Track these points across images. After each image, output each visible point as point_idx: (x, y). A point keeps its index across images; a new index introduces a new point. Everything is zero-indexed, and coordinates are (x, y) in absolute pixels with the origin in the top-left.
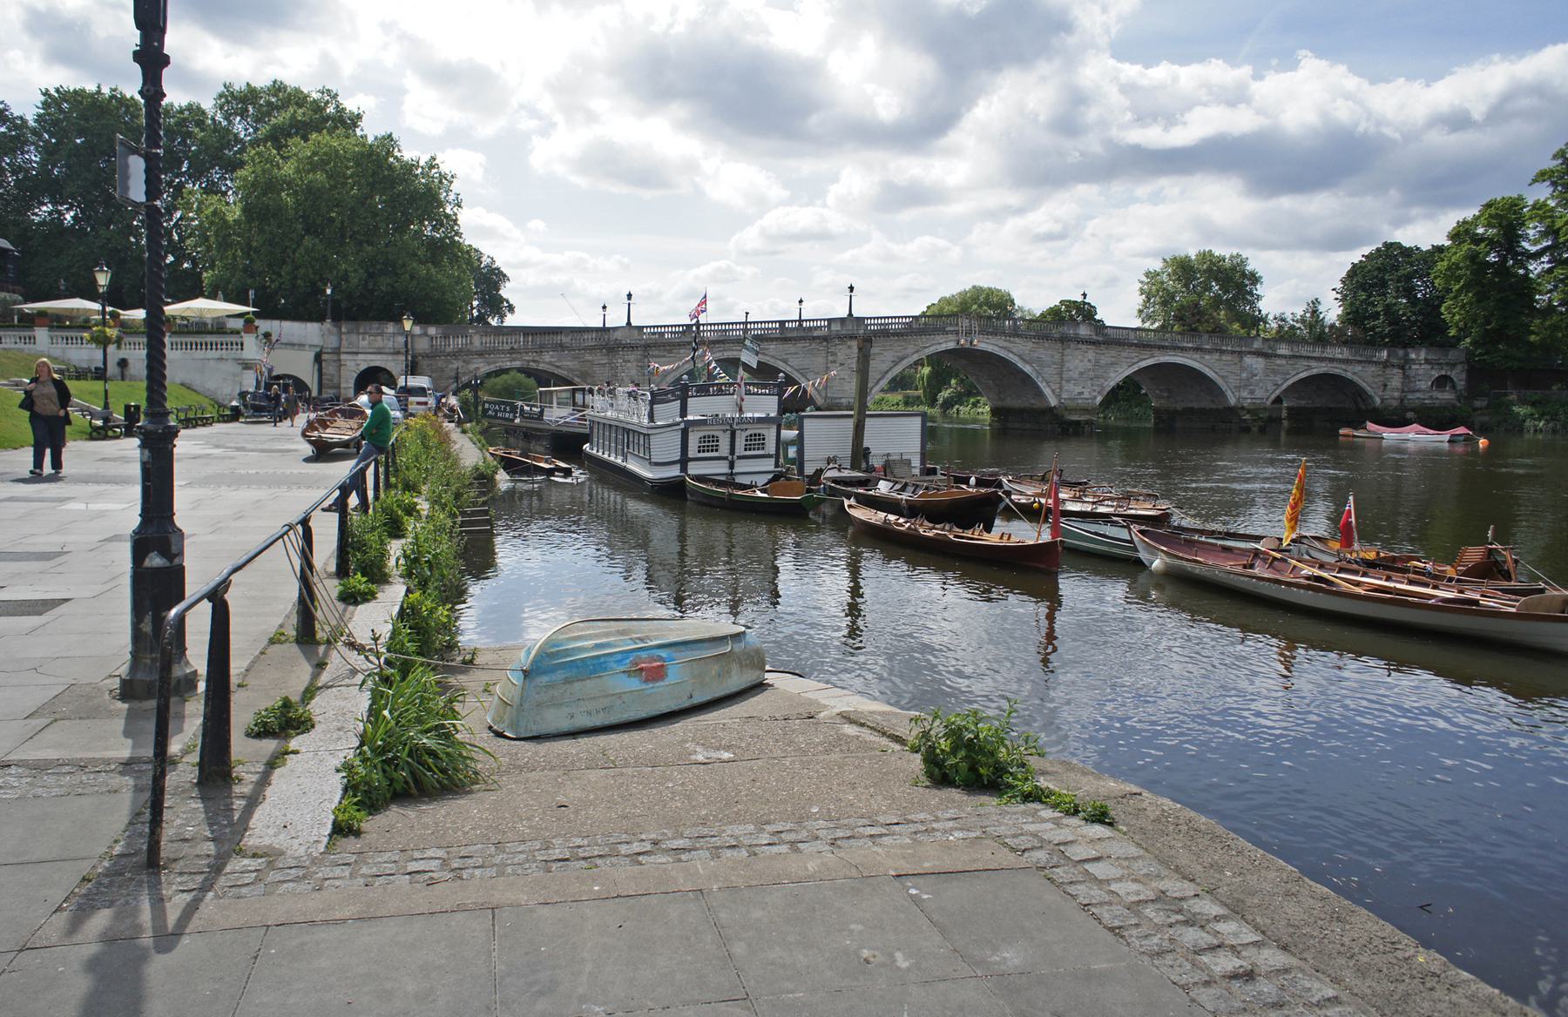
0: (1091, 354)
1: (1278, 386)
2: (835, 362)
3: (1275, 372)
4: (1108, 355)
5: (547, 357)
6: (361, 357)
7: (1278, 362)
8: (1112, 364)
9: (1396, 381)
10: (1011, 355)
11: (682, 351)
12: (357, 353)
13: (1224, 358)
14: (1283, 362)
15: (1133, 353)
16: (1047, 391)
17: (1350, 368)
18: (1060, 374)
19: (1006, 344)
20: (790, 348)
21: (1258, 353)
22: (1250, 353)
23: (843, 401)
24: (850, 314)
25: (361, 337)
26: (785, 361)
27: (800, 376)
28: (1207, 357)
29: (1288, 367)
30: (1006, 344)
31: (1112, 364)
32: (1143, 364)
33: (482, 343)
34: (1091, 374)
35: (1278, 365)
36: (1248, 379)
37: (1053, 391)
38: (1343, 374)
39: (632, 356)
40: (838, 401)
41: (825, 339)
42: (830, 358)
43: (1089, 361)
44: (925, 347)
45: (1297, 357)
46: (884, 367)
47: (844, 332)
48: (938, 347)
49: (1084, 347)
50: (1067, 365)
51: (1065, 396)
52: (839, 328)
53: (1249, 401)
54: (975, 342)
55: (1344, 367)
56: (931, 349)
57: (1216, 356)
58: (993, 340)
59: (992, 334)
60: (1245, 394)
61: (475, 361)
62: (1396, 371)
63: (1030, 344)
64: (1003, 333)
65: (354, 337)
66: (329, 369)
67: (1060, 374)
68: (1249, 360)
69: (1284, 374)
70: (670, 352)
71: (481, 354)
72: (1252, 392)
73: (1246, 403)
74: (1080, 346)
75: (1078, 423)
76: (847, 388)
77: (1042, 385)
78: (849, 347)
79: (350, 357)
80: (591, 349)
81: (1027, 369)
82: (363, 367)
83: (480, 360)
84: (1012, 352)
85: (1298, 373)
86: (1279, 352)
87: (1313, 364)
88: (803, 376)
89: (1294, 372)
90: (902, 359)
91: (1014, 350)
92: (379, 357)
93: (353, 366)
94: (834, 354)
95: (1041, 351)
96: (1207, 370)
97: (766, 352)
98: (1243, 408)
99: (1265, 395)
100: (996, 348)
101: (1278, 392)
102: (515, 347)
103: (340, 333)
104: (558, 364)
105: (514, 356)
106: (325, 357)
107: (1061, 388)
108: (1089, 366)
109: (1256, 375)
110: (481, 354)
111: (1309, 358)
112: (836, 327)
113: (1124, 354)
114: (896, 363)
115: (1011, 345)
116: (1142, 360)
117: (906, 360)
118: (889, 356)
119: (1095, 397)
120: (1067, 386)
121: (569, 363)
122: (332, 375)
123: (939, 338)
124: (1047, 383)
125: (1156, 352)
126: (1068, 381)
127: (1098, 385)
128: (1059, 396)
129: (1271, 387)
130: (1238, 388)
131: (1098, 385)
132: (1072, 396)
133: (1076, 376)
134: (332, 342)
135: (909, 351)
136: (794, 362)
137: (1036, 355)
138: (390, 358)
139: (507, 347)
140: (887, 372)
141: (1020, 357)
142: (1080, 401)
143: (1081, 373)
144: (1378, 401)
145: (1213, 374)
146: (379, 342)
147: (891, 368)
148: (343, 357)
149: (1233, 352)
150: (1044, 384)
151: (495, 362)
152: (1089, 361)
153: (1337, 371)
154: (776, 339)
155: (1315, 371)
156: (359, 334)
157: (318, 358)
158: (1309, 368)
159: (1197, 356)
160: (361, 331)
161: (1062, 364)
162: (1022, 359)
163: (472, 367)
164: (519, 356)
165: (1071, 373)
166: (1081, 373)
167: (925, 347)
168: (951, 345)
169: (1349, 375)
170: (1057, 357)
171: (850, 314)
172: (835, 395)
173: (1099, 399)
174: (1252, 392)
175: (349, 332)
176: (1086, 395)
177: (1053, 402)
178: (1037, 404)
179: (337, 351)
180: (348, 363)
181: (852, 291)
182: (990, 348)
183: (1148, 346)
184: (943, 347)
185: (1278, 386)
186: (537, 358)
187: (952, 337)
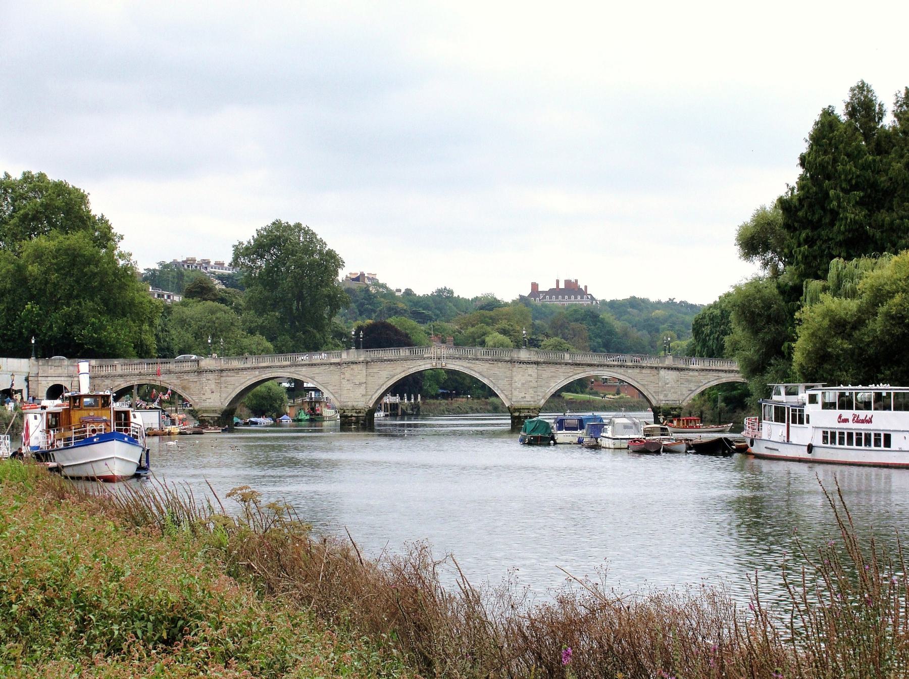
0: (532, 370)
1: (693, 391)
2: (344, 379)
3: (688, 381)
4: (548, 371)
5: (161, 378)
7: (691, 373)
11: (245, 373)
13: (644, 371)
14: (696, 373)
15: (569, 369)
19: (468, 365)
20: (316, 370)
23: (349, 403)
25: (49, 367)
27: (323, 388)
28: (630, 371)
29: (701, 378)
30: (468, 365)
33: (122, 370)
34: (534, 384)
35: (690, 376)
37: (506, 396)
39: (211, 376)
40: (346, 404)
41: (339, 364)
42: (342, 376)
43: (530, 375)
44: (409, 368)
45: (707, 370)
46: (381, 382)
47: (348, 360)
48: (419, 368)
49: (524, 366)
50: (515, 378)
52: (346, 357)
53: (664, 402)
56: (414, 369)
57: (638, 370)
58: (458, 362)
59: (457, 358)
60: (661, 397)
61: (119, 380)
63: (488, 365)
64: (467, 358)
68: (662, 372)
69: (694, 382)
70: (238, 373)
71: (121, 376)
72: (666, 396)
74: (521, 365)
79: (43, 379)
80: (187, 372)
81: (485, 381)
82: (51, 384)
83: (122, 380)
84: (472, 370)
86: (691, 366)
87: (722, 375)
89: (706, 381)
90: (394, 376)
91: (476, 369)
92: (59, 379)
93: (45, 385)
95: (496, 369)
97: (300, 373)
99: (681, 398)
100: (462, 368)
102: (142, 371)
103: (39, 365)
104: (167, 382)
105: (141, 377)
106: (30, 379)
107: (512, 394)
108: (529, 379)
109: (668, 384)
110: (121, 376)
111: (716, 370)
113: (561, 370)
114: (389, 379)
115: (472, 366)
117: (396, 377)
118: (384, 374)
119: (540, 400)
120: (516, 393)
121: (175, 381)
122: (34, 389)
124: (502, 391)
125: (588, 369)
127: (542, 392)
129: (686, 392)
131: (542, 392)
132: (518, 400)
134: (34, 371)
135: (398, 371)
136: (318, 378)
138: (66, 379)
139: (137, 372)
141: (478, 373)
142: (523, 403)
143: (523, 384)
146: (59, 371)
148: (40, 379)
150: (500, 391)
151: (130, 381)
152: (530, 375)
154: (305, 365)
155: (724, 380)
156: (48, 365)
157: (27, 380)
159: (622, 370)
160: (50, 364)
161: (512, 377)
163: (117, 383)
164: (144, 377)
165: (516, 384)
166: (523, 384)
167: (409, 368)
172: (345, 400)
173: (543, 402)
174: (666, 396)
175: (43, 365)
176: (528, 398)
179: (37, 375)
180: (43, 382)
182: (457, 368)
183: (582, 365)
185: (693, 391)
186: (155, 378)
187: (428, 361)
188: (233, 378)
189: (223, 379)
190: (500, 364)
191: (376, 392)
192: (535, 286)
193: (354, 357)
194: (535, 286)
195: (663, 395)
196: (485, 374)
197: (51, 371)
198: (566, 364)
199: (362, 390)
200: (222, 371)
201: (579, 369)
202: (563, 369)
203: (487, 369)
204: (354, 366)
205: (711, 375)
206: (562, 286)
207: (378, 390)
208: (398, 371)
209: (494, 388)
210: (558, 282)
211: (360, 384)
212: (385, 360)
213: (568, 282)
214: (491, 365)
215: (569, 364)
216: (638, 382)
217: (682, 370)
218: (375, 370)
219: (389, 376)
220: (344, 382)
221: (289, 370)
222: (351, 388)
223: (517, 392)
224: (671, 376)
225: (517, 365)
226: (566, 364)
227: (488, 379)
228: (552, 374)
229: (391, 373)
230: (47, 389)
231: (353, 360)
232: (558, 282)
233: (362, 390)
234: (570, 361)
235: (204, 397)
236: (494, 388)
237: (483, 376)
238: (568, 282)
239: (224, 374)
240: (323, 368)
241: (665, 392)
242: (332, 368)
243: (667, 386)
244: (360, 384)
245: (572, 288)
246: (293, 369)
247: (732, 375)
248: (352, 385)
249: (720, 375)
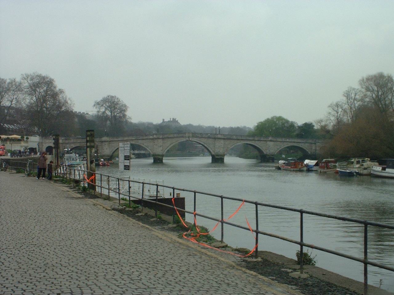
0: (222, 141)
2: (154, 144)
6: (47, 144)
9: (314, 148)
12: (46, 143)
13: (262, 142)
17: (300, 144)
18: (214, 146)
20: (144, 141)
21: (271, 141)
22: (269, 141)
26: (143, 144)
28: (257, 142)
30: (199, 140)
37: (213, 151)
38: (298, 146)
39: (106, 143)
42: (154, 143)
43: (222, 143)
51: (216, 152)
54: (191, 139)
55: (299, 144)
57: (259, 142)
58: (195, 138)
60: (268, 151)
62: (314, 145)
65: (45, 140)
66: (40, 147)
68: (268, 142)
73: (268, 153)
75: (218, 158)
78: (158, 141)
79: (44, 144)
87: (289, 143)
90: (172, 143)
94: (154, 142)
101: (278, 151)
114: (171, 144)
116: (237, 143)
123: (182, 138)
125: (242, 141)
126: (216, 148)
128: (214, 152)
130: (266, 149)
139: (79, 142)
140: (169, 146)
143: (219, 146)
144: (309, 153)
148: (43, 144)
149: (264, 141)
152: (222, 143)
153: (296, 145)
155: (289, 145)
158: (288, 144)
159: (254, 142)
163: (71, 146)
168: (185, 140)
169: (300, 146)
179: (42, 143)
184: (183, 141)
185: (279, 149)
187: (185, 138)
188: (114, 144)
189: (110, 144)
190: (211, 139)
191: (166, 149)
192: (163, 120)
194: (163, 120)
197: (47, 141)
198: (234, 139)
199: (161, 148)
200: (110, 141)
201: (239, 141)
202: (233, 141)
204: (159, 140)
205: (285, 143)
206: (172, 120)
210: (170, 119)
211: (161, 146)
212: (170, 138)
213: (173, 119)
215: (235, 139)
217: (275, 141)
218: (166, 141)
221: (134, 141)
224: (271, 144)
225: (217, 140)
226: (234, 139)
227: (206, 144)
230: (46, 148)
232: (170, 119)
233: (161, 148)
234: (235, 138)
235: (104, 151)
237: (205, 144)
238: (173, 119)
239: (111, 142)
240: (147, 140)
242: (150, 140)
244: (161, 146)
245: (174, 121)
246: (136, 141)
247: (292, 143)
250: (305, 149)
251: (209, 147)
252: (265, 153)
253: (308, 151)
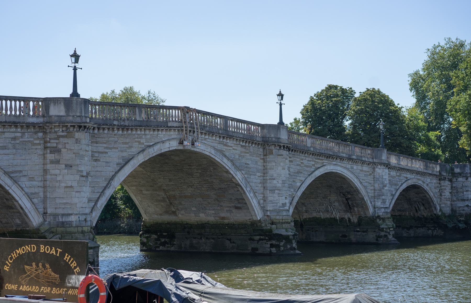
2: (58, 162)
8: (299, 172)
9: (447, 193)
10: (225, 160)
16: (254, 203)
19: (220, 147)
21: (388, 166)
22: (381, 164)
23: (73, 219)
24: (75, 94)
28: (355, 167)
30: (220, 147)
31: (299, 172)
32: (318, 173)
36: (380, 190)
37: (259, 203)
42: (50, 157)
44: (150, 146)
46: (110, 172)
50: (271, 172)
52: (63, 113)
53: (383, 210)
55: (422, 179)
56: (156, 148)
60: (379, 204)
63: (239, 148)
67: (264, 182)
76: (75, 200)
77: (250, 195)
78: (78, 141)
81: (239, 177)
84: (225, 156)
85: (402, 184)
87: (409, 176)
88: (15, 182)
91: (227, 154)
94: (56, 150)
96: (356, 180)
98: (379, 216)
100: (213, 152)
112: (55, 111)
115: (224, 148)
117: (131, 163)
120: (271, 197)
124: (254, 193)
126: (273, 191)
133: (279, 185)
137: (244, 161)
141: (232, 161)
144: (438, 208)
145: (359, 185)
147: (117, 173)
150: (252, 195)
155: (410, 183)
161: (265, 171)
162: (233, 164)
165: (275, 182)
168: (174, 145)
169: (425, 187)
170: (260, 163)
171: (75, 94)
172: (60, 211)
177: (259, 215)
178: (255, 218)
181: (77, 61)
187: (174, 134)
193: (81, 113)
195: (380, 201)
196: (238, 164)
201: (319, 162)
203: (240, 156)
207: (105, 188)
208: (134, 150)
209: (246, 188)
214: (243, 150)
216: (361, 183)
218: (101, 148)
219: (121, 161)
220: (53, 170)
222: (75, 184)
223: (276, 195)
228: (298, 167)
229: (125, 154)
231: (78, 120)
236: (246, 188)
241: (383, 197)
243: (385, 188)
248: (77, 177)
249: (408, 176)
250: (431, 194)
251: (247, 182)
252: (371, 210)
253: (435, 202)
